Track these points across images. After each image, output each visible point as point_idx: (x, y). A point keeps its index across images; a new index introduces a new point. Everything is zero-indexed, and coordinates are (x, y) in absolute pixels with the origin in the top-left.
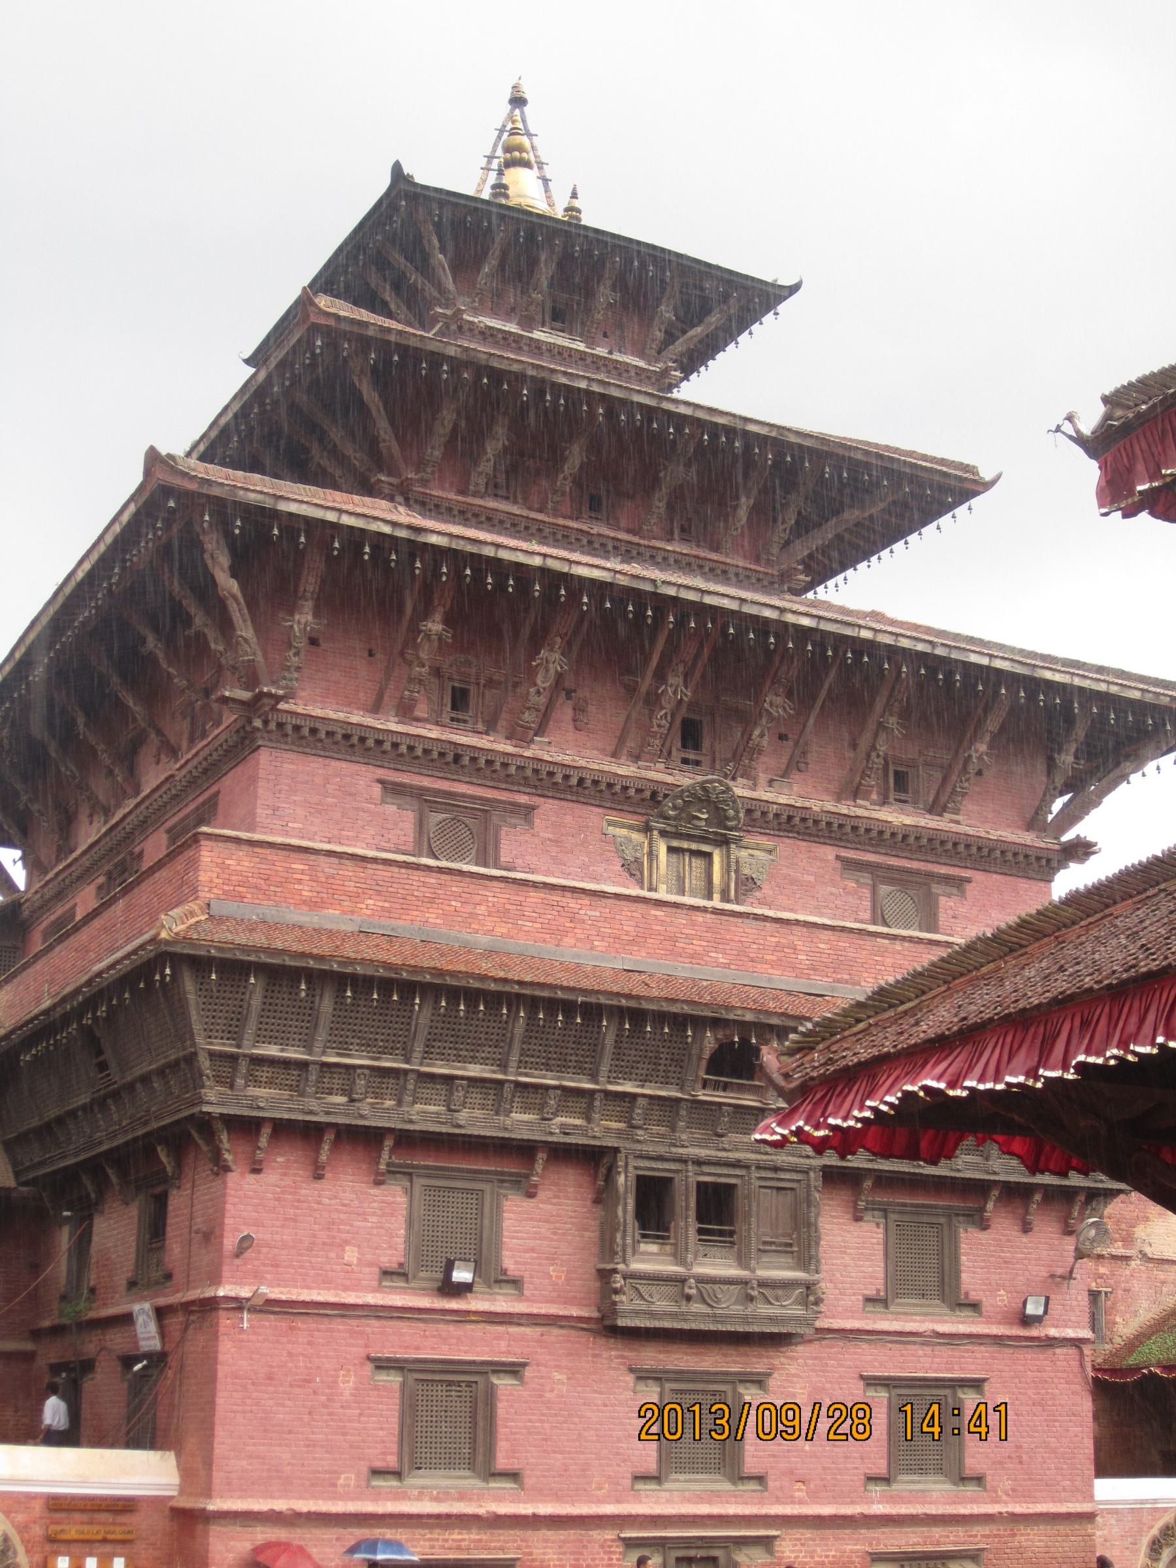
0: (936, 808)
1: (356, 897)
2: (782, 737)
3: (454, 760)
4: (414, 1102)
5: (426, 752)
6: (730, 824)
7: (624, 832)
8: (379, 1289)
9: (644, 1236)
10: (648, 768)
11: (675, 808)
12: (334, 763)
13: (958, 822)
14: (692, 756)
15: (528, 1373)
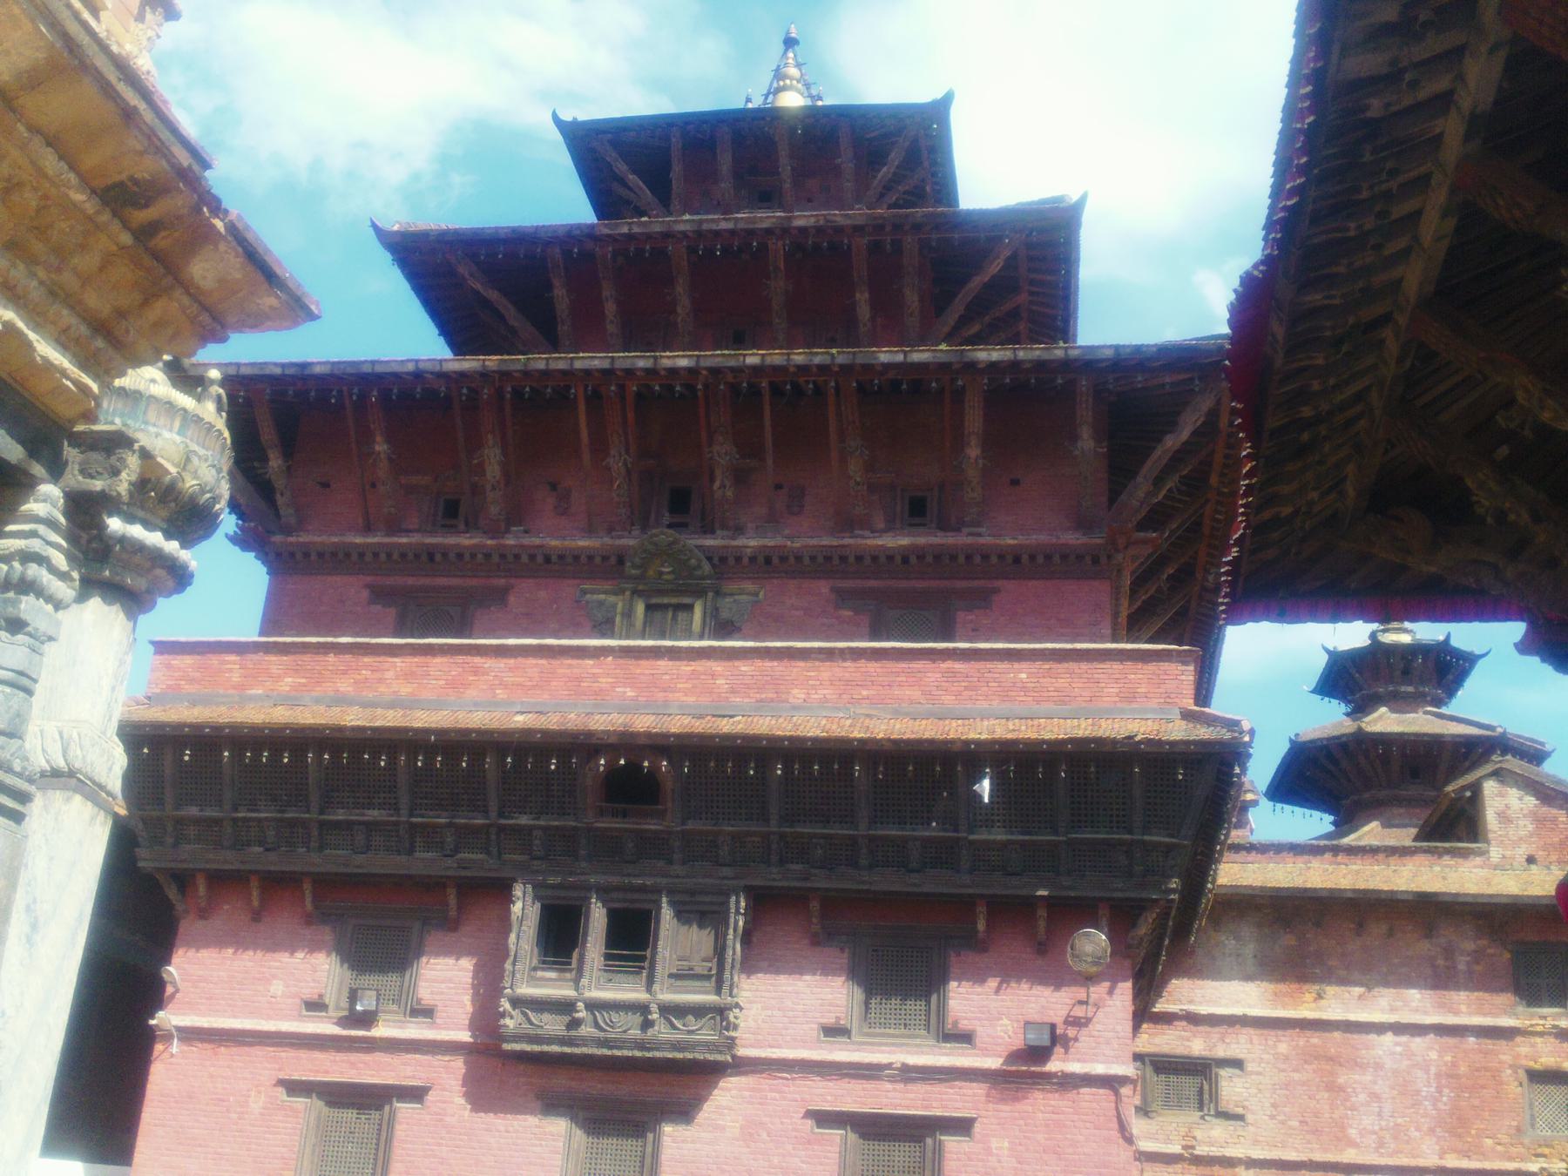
0: (944, 526)
1: (279, 678)
2: (778, 487)
3: (430, 558)
4: (321, 848)
5: (403, 555)
6: (699, 573)
7: (602, 597)
8: (300, 1017)
9: (544, 962)
10: (620, 537)
11: (634, 566)
12: (330, 579)
13: (980, 535)
14: (677, 519)
15: (430, 1097)
